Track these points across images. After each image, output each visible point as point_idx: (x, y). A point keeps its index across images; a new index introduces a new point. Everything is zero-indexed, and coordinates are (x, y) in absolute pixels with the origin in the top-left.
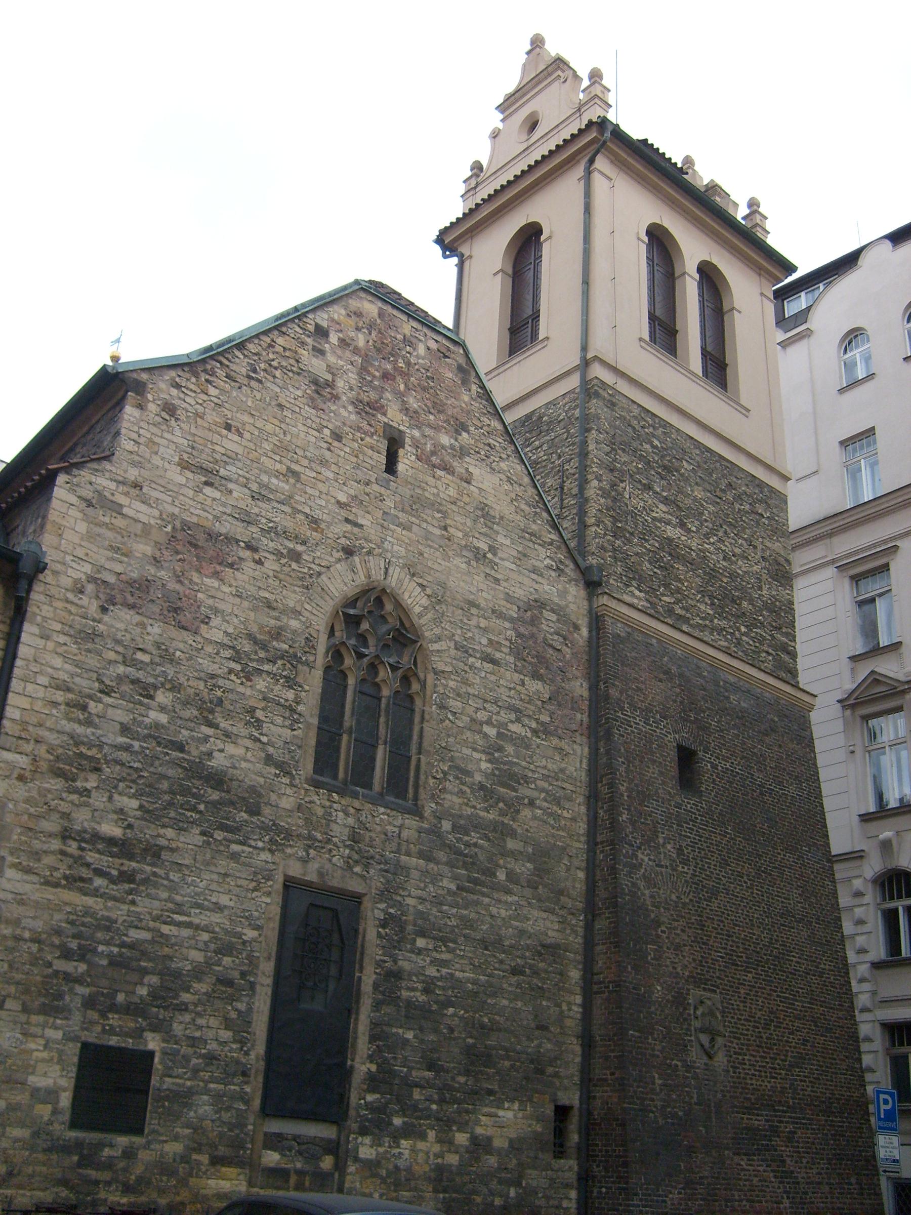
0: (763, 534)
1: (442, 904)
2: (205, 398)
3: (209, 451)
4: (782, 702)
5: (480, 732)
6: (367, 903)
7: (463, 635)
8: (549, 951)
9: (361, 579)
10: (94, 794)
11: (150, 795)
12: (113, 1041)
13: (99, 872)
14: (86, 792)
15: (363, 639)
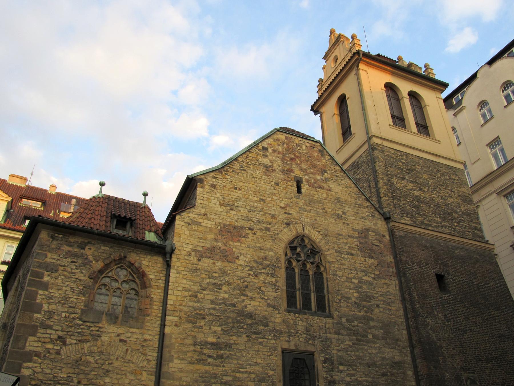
1: (347, 351)
2: (226, 180)
4: (480, 250)
5: (351, 282)
7: (338, 246)
8: (398, 364)
9: (294, 233)
10: (204, 327)
11: (225, 325)
13: (209, 356)
14: (201, 327)
15: (298, 255)
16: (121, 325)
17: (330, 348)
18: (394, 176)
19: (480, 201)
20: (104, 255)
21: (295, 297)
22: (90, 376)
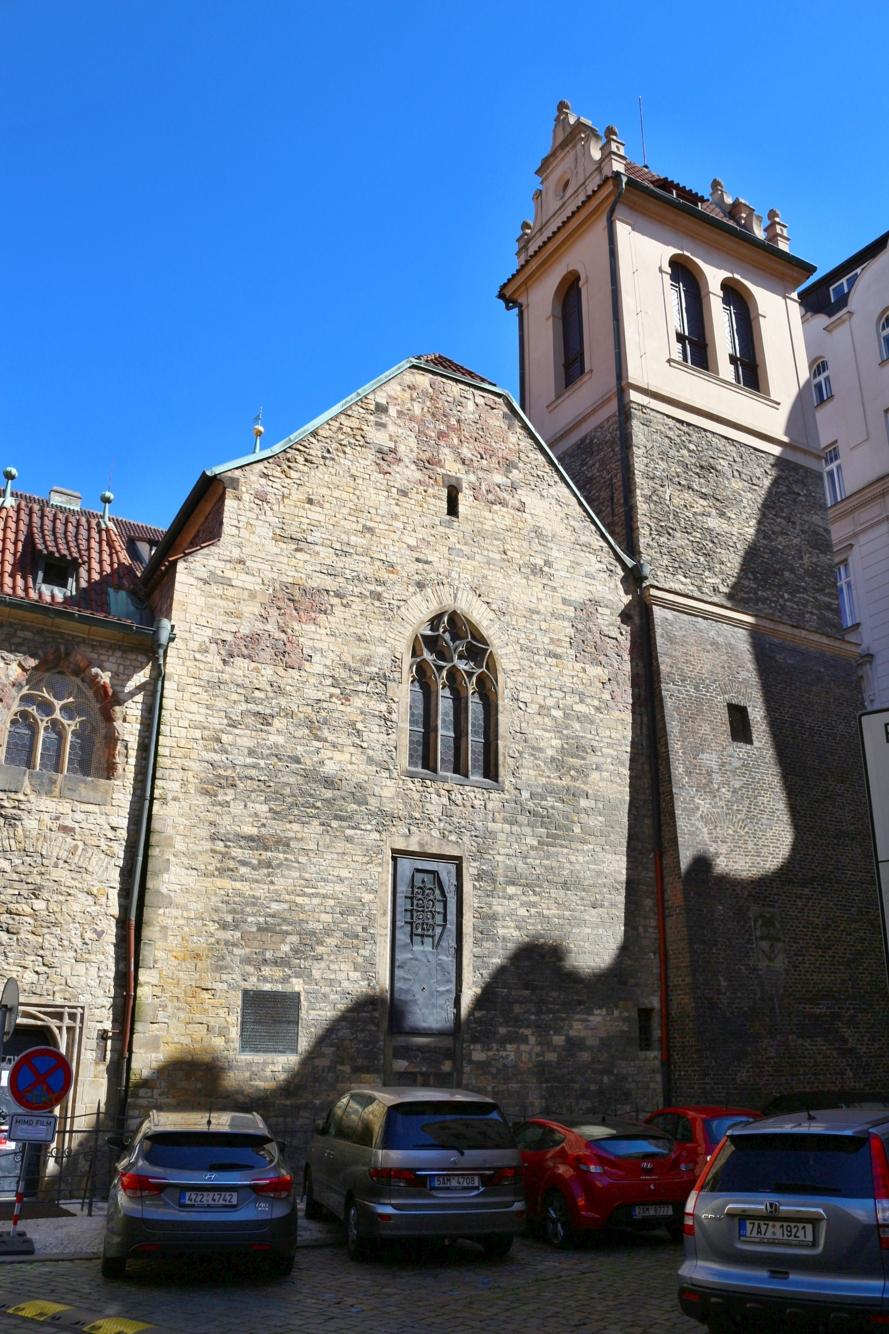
0: (801, 511)
2: (288, 481)
3: (297, 524)
11: (276, 800)
12: (267, 987)
13: (244, 863)
17: (491, 852)
19: (856, 535)
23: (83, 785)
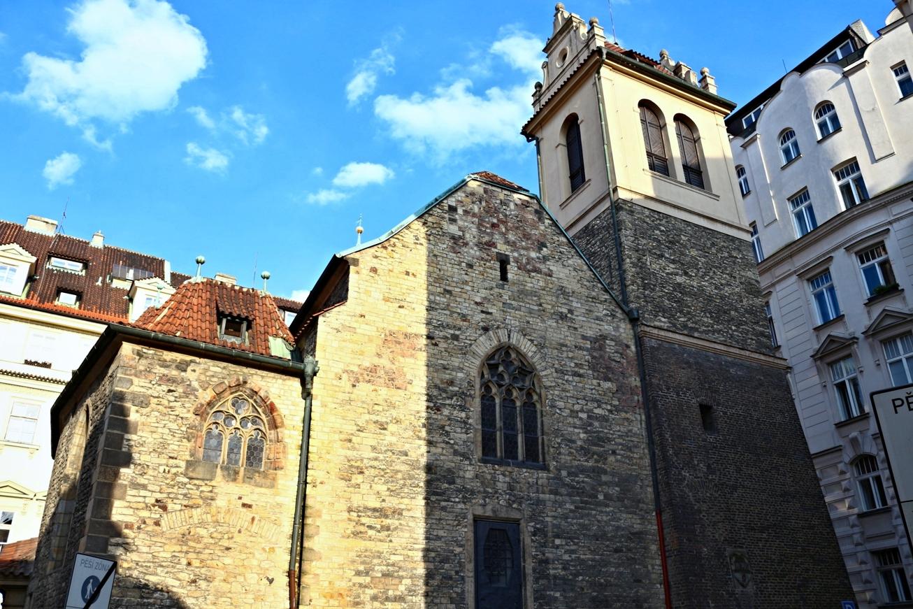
1: (567, 518)
2: (392, 260)
3: (398, 289)
5: (577, 417)
6: (523, 523)
8: (639, 536)
9: (495, 343)
11: (393, 482)
13: (370, 527)
14: (358, 486)
15: (501, 376)
16: (244, 482)
18: (647, 253)
19: (773, 285)
20: (215, 379)
21: (495, 440)
22: (202, 556)
23: (257, 475)
